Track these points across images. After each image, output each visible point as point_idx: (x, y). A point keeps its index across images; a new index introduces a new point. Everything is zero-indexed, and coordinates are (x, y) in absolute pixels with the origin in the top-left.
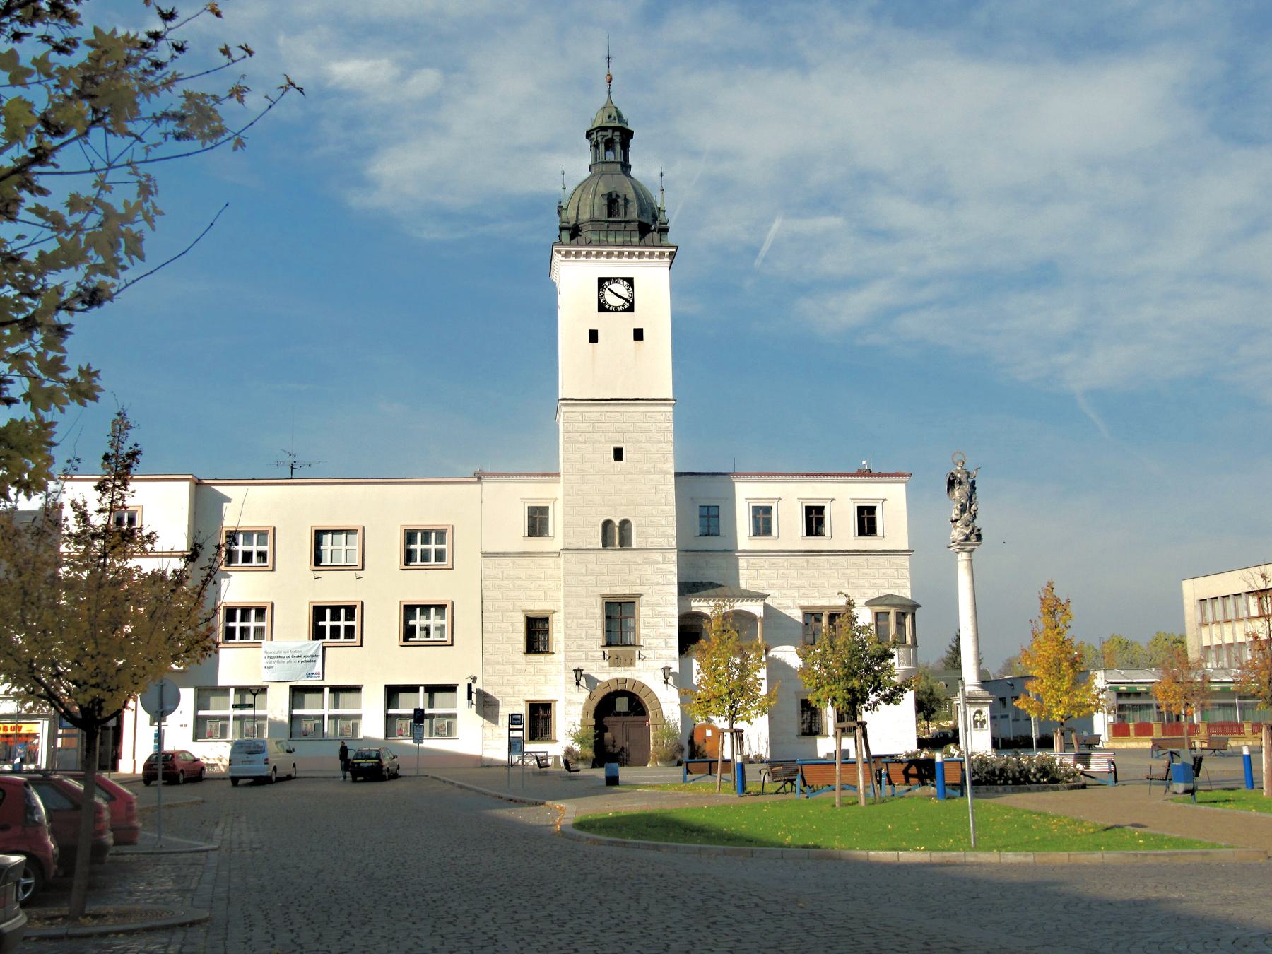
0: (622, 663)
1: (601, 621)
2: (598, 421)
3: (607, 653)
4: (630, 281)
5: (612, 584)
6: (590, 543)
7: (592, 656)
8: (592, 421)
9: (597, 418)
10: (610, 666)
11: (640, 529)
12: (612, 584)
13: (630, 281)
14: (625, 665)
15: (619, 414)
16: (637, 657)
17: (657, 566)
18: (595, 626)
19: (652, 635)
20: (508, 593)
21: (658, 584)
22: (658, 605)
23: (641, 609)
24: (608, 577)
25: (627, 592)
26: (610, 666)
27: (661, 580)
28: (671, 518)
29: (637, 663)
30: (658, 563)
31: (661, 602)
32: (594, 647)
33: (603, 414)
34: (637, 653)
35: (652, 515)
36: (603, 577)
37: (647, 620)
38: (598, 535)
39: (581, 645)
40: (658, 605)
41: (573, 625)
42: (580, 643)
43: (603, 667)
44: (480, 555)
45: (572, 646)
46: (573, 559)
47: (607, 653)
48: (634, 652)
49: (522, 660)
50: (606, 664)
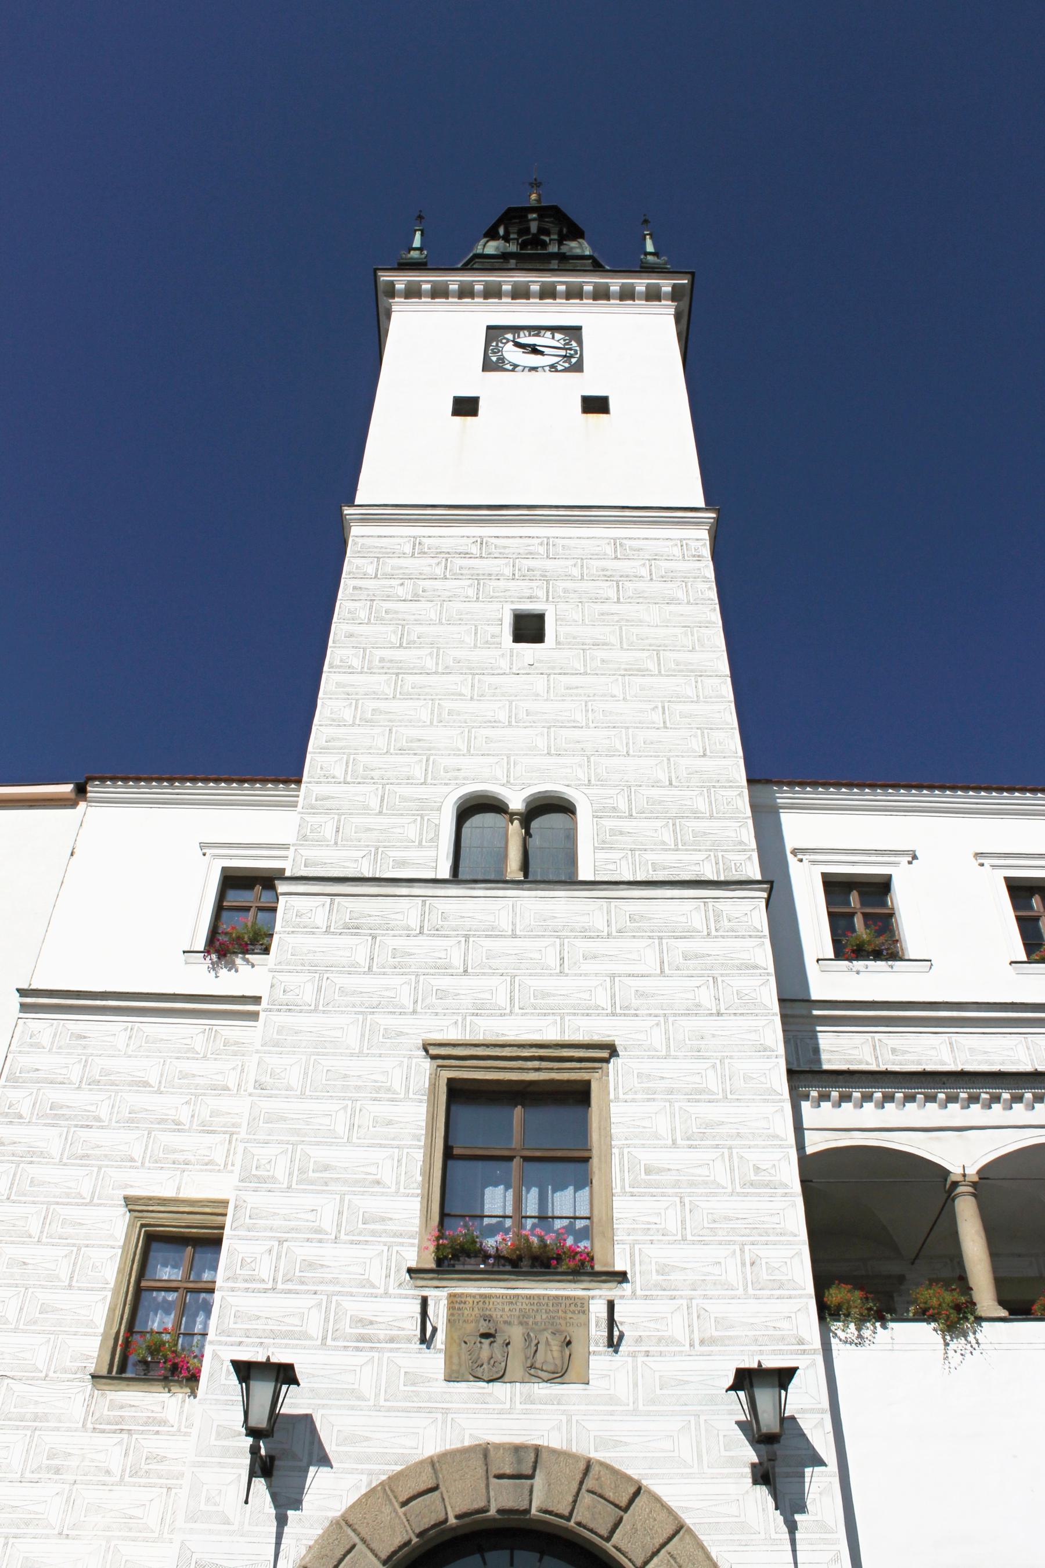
0: (516, 1365)
1: (419, 1155)
2: (466, 555)
3: (438, 1314)
4: (574, 332)
5: (479, 1010)
6: (402, 864)
7: (361, 1322)
8: (445, 556)
9: (461, 549)
10: (451, 1377)
11: (608, 823)
12: (479, 1010)
13: (574, 332)
14: (533, 1372)
15: (536, 541)
16: (598, 1332)
17: (682, 945)
18: (387, 1175)
19: (672, 1224)
20: (83, 1133)
21: (693, 1011)
22: (698, 1094)
23: (614, 1108)
24: (465, 981)
25: (551, 1034)
26: (451, 1377)
27: (706, 998)
28: (732, 793)
29: (600, 1361)
30: (688, 934)
31: (712, 1082)
32: (376, 1274)
33: (481, 542)
34: (598, 1310)
35: (656, 784)
36: (443, 982)
37: (646, 1157)
38: (436, 838)
39: (311, 1265)
40: (698, 1094)
41: (280, 1171)
42: (305, 1251)
43: (412, 1379)
44: (17, 1000)
45: (265, 1271)
46: (320, 918)
47: (438, 1314)
48: (581, 1307)
49: (77, 1410)
50: (434, 1362)
